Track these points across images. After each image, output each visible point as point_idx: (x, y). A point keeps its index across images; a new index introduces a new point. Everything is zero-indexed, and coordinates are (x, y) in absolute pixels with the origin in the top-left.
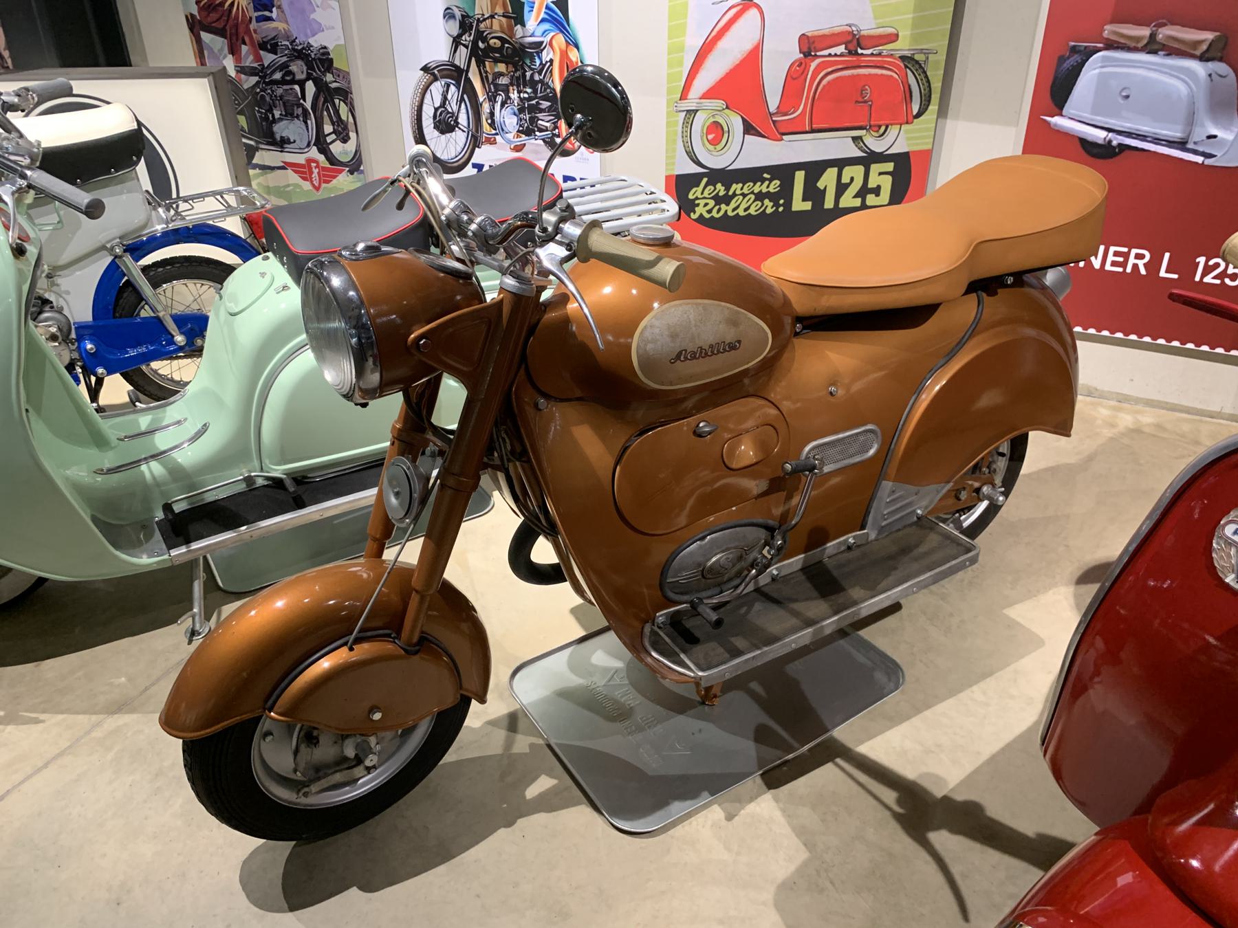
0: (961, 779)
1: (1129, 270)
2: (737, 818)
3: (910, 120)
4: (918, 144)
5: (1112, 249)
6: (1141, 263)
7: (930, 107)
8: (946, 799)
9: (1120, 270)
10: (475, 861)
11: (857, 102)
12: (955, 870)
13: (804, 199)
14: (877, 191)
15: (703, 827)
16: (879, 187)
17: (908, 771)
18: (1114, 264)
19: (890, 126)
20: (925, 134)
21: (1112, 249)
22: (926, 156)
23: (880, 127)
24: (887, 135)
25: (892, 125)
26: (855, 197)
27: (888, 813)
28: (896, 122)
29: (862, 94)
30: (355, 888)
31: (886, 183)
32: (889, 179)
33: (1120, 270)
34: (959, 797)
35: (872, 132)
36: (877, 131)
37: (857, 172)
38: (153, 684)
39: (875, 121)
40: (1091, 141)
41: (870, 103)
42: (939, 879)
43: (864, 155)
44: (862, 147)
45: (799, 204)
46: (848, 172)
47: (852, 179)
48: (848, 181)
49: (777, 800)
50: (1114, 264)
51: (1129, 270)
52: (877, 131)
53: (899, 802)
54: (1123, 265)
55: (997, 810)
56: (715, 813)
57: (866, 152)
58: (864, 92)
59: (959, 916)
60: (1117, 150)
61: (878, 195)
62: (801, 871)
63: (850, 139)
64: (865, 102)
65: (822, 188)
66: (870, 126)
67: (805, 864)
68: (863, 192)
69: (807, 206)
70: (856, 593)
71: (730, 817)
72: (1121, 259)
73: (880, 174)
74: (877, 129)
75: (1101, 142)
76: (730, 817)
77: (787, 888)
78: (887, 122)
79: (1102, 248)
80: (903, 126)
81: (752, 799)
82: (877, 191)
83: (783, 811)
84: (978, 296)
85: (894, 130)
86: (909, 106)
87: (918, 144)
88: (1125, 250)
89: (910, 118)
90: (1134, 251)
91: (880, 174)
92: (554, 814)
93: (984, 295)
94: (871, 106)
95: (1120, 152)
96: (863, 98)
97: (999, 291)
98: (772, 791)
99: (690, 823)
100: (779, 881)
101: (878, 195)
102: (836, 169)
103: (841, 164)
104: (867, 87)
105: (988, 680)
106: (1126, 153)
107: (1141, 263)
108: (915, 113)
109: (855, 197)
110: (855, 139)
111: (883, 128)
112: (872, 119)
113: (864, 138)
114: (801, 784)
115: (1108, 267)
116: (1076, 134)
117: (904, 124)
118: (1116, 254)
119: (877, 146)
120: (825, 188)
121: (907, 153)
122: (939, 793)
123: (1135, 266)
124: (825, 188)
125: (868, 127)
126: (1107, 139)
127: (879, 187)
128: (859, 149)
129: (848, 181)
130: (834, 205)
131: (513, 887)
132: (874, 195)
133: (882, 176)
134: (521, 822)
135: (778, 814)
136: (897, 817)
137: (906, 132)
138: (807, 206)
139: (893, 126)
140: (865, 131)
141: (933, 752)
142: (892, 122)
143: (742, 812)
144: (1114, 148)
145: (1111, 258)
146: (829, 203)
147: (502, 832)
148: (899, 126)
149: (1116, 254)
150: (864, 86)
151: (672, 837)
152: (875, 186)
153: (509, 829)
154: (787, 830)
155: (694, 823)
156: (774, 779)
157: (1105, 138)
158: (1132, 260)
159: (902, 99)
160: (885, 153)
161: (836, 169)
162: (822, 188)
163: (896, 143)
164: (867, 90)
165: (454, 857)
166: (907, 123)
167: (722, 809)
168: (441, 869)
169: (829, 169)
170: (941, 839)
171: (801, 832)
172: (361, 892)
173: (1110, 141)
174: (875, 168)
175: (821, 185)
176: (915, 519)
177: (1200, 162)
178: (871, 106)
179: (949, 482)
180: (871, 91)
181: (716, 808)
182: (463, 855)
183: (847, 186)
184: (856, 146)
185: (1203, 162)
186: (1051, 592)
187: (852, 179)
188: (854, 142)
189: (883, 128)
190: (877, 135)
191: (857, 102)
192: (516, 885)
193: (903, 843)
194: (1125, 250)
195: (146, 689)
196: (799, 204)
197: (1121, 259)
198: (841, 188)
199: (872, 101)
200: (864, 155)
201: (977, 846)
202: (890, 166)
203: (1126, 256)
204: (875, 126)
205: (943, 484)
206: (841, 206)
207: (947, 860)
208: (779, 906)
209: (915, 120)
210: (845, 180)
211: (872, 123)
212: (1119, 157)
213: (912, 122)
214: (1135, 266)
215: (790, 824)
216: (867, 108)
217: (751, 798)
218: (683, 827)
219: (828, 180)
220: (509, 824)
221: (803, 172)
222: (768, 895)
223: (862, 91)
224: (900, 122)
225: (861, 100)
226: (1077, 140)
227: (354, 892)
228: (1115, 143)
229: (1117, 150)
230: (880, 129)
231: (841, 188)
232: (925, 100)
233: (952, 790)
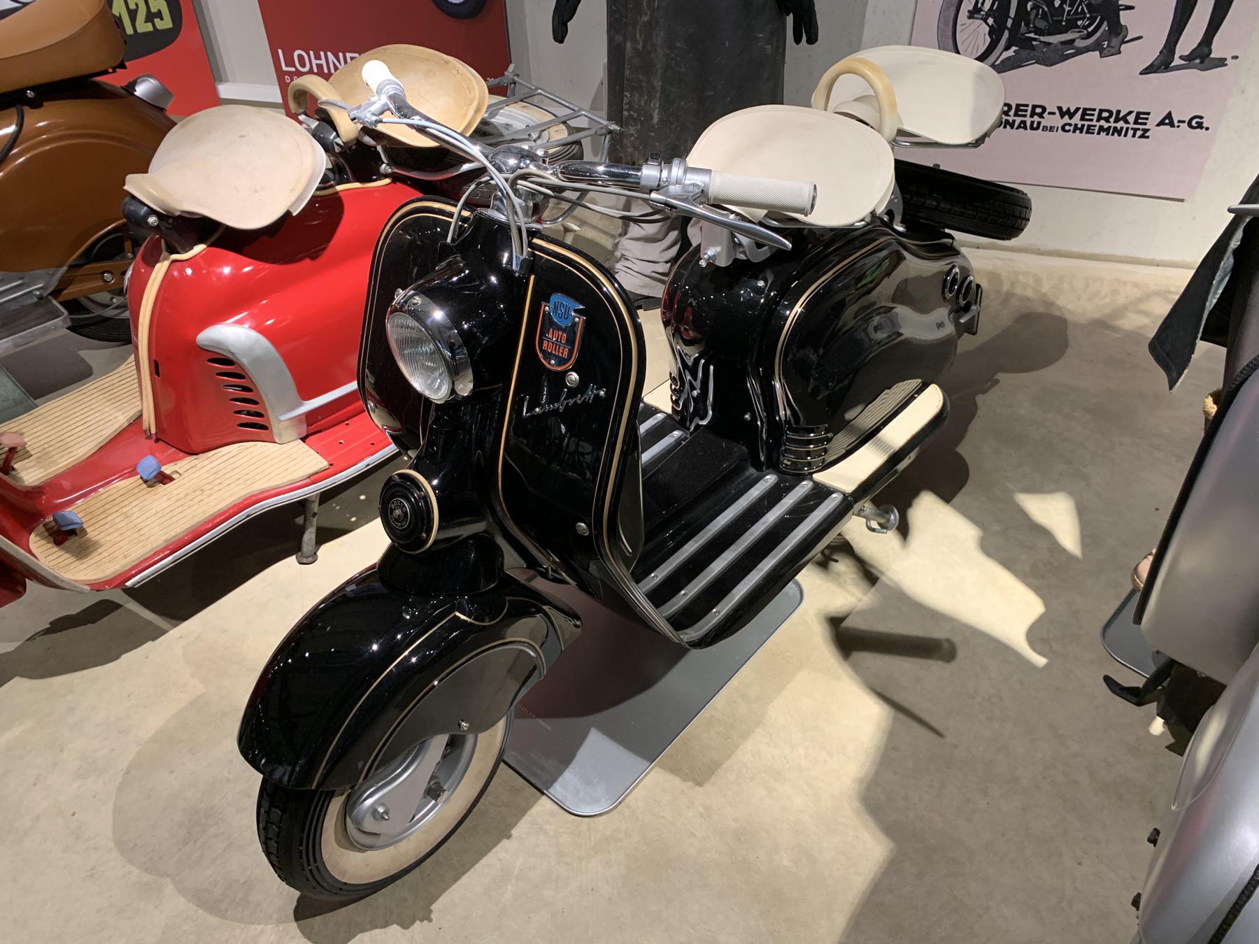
14: (159, 14)
16: (160, 11)
47: (137, 5)
84: (17, 109)
93: (26, 109)
97: (44, 103)
146: (130, 31)
162: (117, 15)
176: (36, 300)
179: (62, 266)
187: (137, 5)
205: (53, 269)
210: (132, 7)
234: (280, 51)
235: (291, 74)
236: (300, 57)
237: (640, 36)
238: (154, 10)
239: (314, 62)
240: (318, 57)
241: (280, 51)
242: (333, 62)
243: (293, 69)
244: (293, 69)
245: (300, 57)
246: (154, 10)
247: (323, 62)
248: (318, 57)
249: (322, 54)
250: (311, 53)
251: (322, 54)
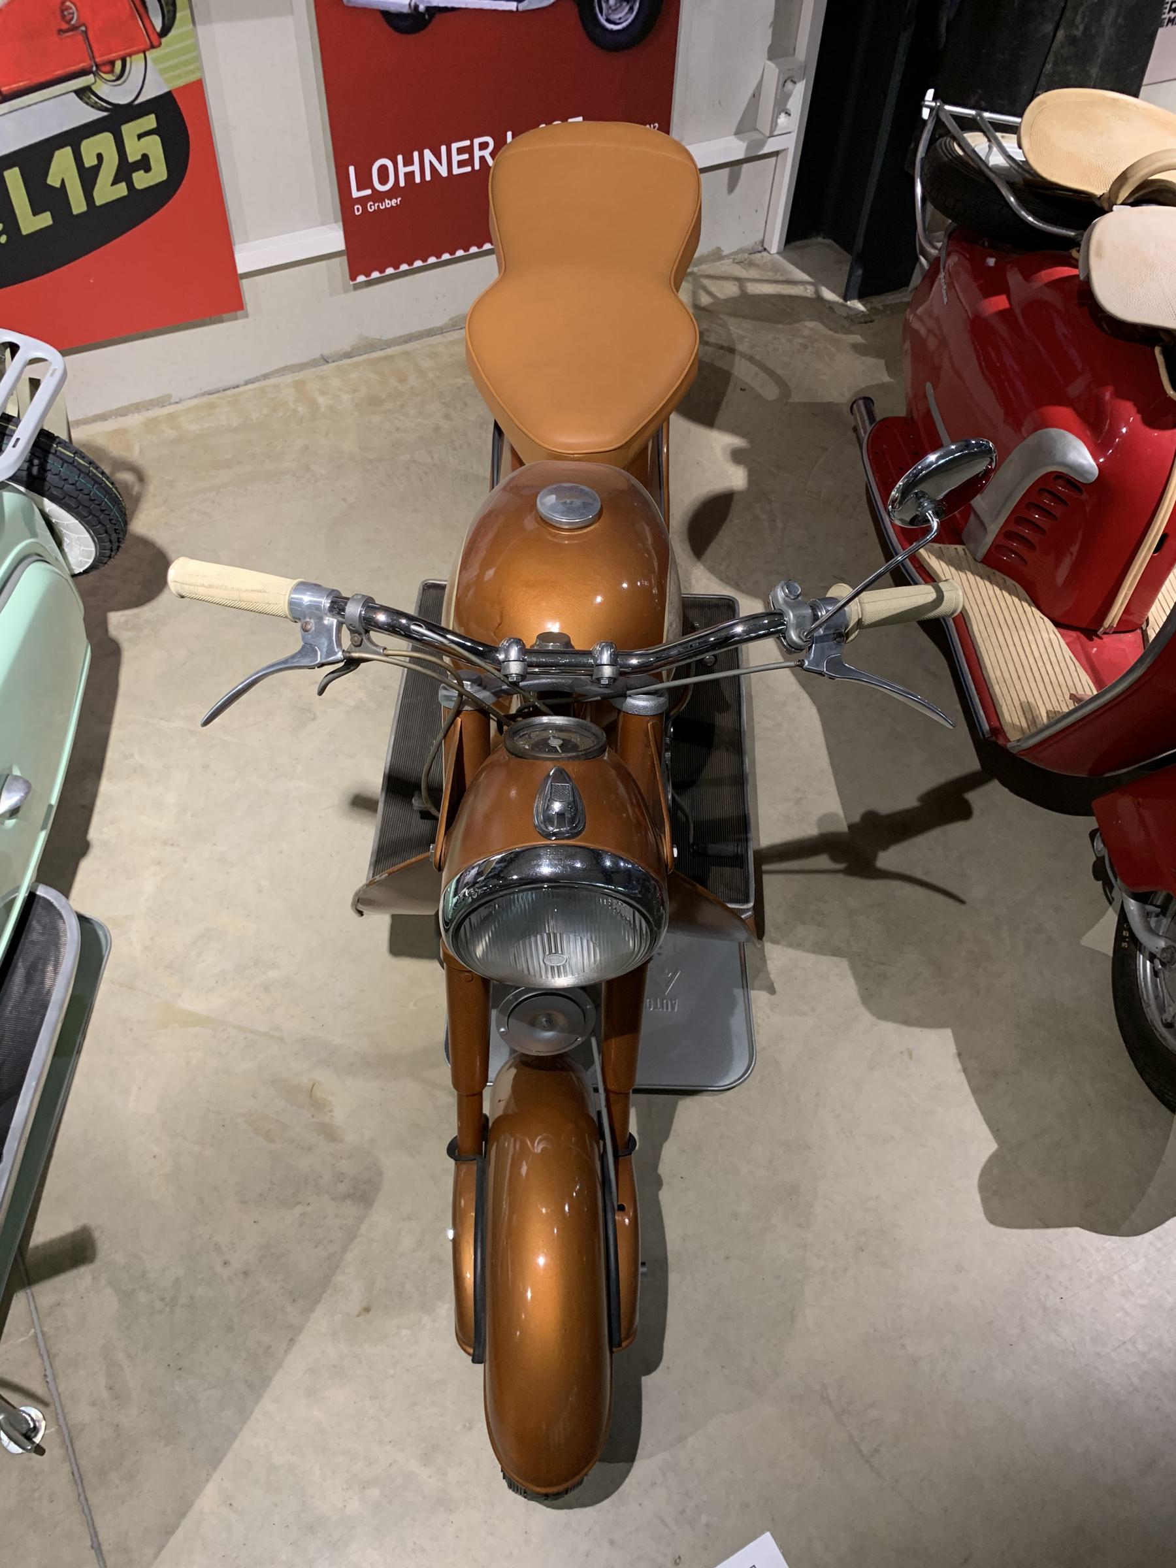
0: (839, 802)
1: (477, 167)
2: (775, 984)
3: (155, 43)
4: (179, 76)
5: (455, 146)
6: (486, 153)
7: (178, 15)
8: (851, 827)
9: (468, 169)
10: (684, 1240)
11: (60, 31)
12: (919, 874)
13: (35, 213)
14: (144, 164)
15: (768, 1017)
16: (145, 157)
17: (810, 830)
18: (461, 164)
19: (128, 59)
20: (183, 58)
21: (455, 146)
22: (197, 89)
23: (112, 63)
24: (129, 74)
25: (130, 55)
26: (114, 184)
27: (840, 876)
28: (135, 49)
29: (63, 17)
30: (643, 1378)
31: (154, 147)
32: (156, 139)
33: (468, 169)
34: (856, 818)
35: (102, 75)
36: (112, 72)
37: (103, 143)
38: (94, 1534)
39: (101, 56)
40: (395, 12)
41: (83, 28)
42: (921, 892)
43: (105, 114)
44: (96, 102)
45: (31, 222)
46: (90, 148)
47: (100, 157)
48: (95, 162)
49: (775, 942)
50: (461, 164)
51: (477, 167)
52: (112, 72)
53: (834, 859)
54: (470, 162)
55: (887, 805)
56: (759, 997)
57: (105, 110)
58: (66, 13)
59: (958, 904)
60: (427, 17)
61: (148, 169)
62: (858, 978)
63: (73, 95)
64: (74, 28)
65: (58, 185)
66: (97, 66)
67: (853, 968)
68: (125, 171)
69: (45, 220)
70: (723, 721)
71: (772, 990)
72: (466, 156)
73: (140, 136)
74: (108, 68)
75: (406, 10)
76: (772, 990)
77: (868, 998)
78: (122, 53)
79: (444, 148)
80: (147, 53)
81: (763, 959)
82: (144, 164)
83: (790, 945)
85: (136, 64)
86: (146, 21)
87: (179, 76)
88: (467, 143)
89: (154, 38)
90: (477, 141)
91: (140, 136)
92: (672, 1134)
94: (86, 32)
95: (431, 17)
96: (68, 22)
98: (764, 939)
99: (759, 1025)
100: (858, 999)
101: (148, 169)
102: (68, 150)
103: (73, 138)
104: (68, 3)
105: (754, 703)
106: (438, 17)
107: (486, 153)
108: (158, 29)
109: (114, 184)
110: (82, 93)
111: (118, 64)
112: (96, 54)
113: (94, 88)
114: (771, 914)
115: (456, 171)
116: (375, 7)
117: (148, 50)
118: (460, 151)
119: (120, 95)
120: (63, 181)
121: (169, 94)
122: (843, 827)
123: (482, 158)
124: (63, 181)
125: (94, 69)
126: (413, 4)
127: (145, 157)
128: (92, 107)
129: (95, 162)
130: (88, 205)
131: (737, 1219)
132: (142, 172)
133: (143, 140)
134: (663, 1170)
135: (791, 952)
136: (848, 872)
137: (156, 61)
138: (45, 220)
139: (134, 57)
140: (92, 76)
141: (800, 799)
142: (128, 51)
143: (772, 976)
144: (422, 14)
145: (456, 158)
146: (78, 206)
147: (664, 1196)
148: (142, 55)
149: (460, 151)
150: (63, 3)
151: (764, 1049)
152: (139, 157)
153: (664, 1187)
154: (812, 957)
155: (759, 1021)
156: (759, 928)
157: (410, 5)
158: (477, 154)
159: (131, 8)
160: (137, 102)
161: (68, 150)
162: (58, 185)
163: (146, 82)
164: (71, 8)
165: (666, 1258)
166: (153, 47)
167: (759, 990)
168: (673, 1278)
169: (57, 153)
170: (887, 859)
171: (821, 948)
172: (654, 1374)
173: (416, 7)
174: (129, 130)
175: (53, 180)
177: (515, 9)
178: (86, 32)
180: (77, 10)
181: (754, 994)
182: (669, 1248)
183: (97, 169)
184: (87, 103)
185: (517, 8)
186: (693, 582)
187: (100, 157)
188: (81, 99)
189: (118, 64)
190: (114, 78)
191: (60, 31)
192: (735, 1216)
193: (876, 887)
194: (467, 143)
195: (97, 1547)
196: (31, 222)
197: (466, 156)
198: (88, 177)
199: (84, 25)
200: (105, 114)
201: (905, 844)
202: (150, 121)
203: (469, 150)
204: (104, 64)
206: (98, 203)
207: (908, 872)
208: (882, 1014)
209: (164, 40)
210: (89, 161)
211: (98, 60)
212: (431, 26)
213: (160, 44)
214: (482, 158)
215: (807, 951)
216: (80, 38)
217: (761, 959)
218: (758, 1033)
219: (62, 169)
220: (658, 1183)
221: (16, 170)
222: (866, 1017)
223: (62, 11)
224: (142, 47)
225: (65, 26)
226: (379, 15)
227: (647, 1381)
228: (422, 8)
229: (427, 17)
230: (115, 68)
231: (88, 177)
232: (167, 4)
233: (845, 817)
234: (352, 169)
235: (363, 201)
236: (383, 170)
237: (1083, 19)
238: (133, 156)
239: (402, 170)
240: (408, 162)
241: (352, 169)
242: (431, 162)
243: (369, 192)
244: (369, 192)
245: (383, 170)
246: (133, 156)
247: (416, 168)
248: (408, 162)
249: (416, 154)
250: (400, 158)
251: (416, 154)
